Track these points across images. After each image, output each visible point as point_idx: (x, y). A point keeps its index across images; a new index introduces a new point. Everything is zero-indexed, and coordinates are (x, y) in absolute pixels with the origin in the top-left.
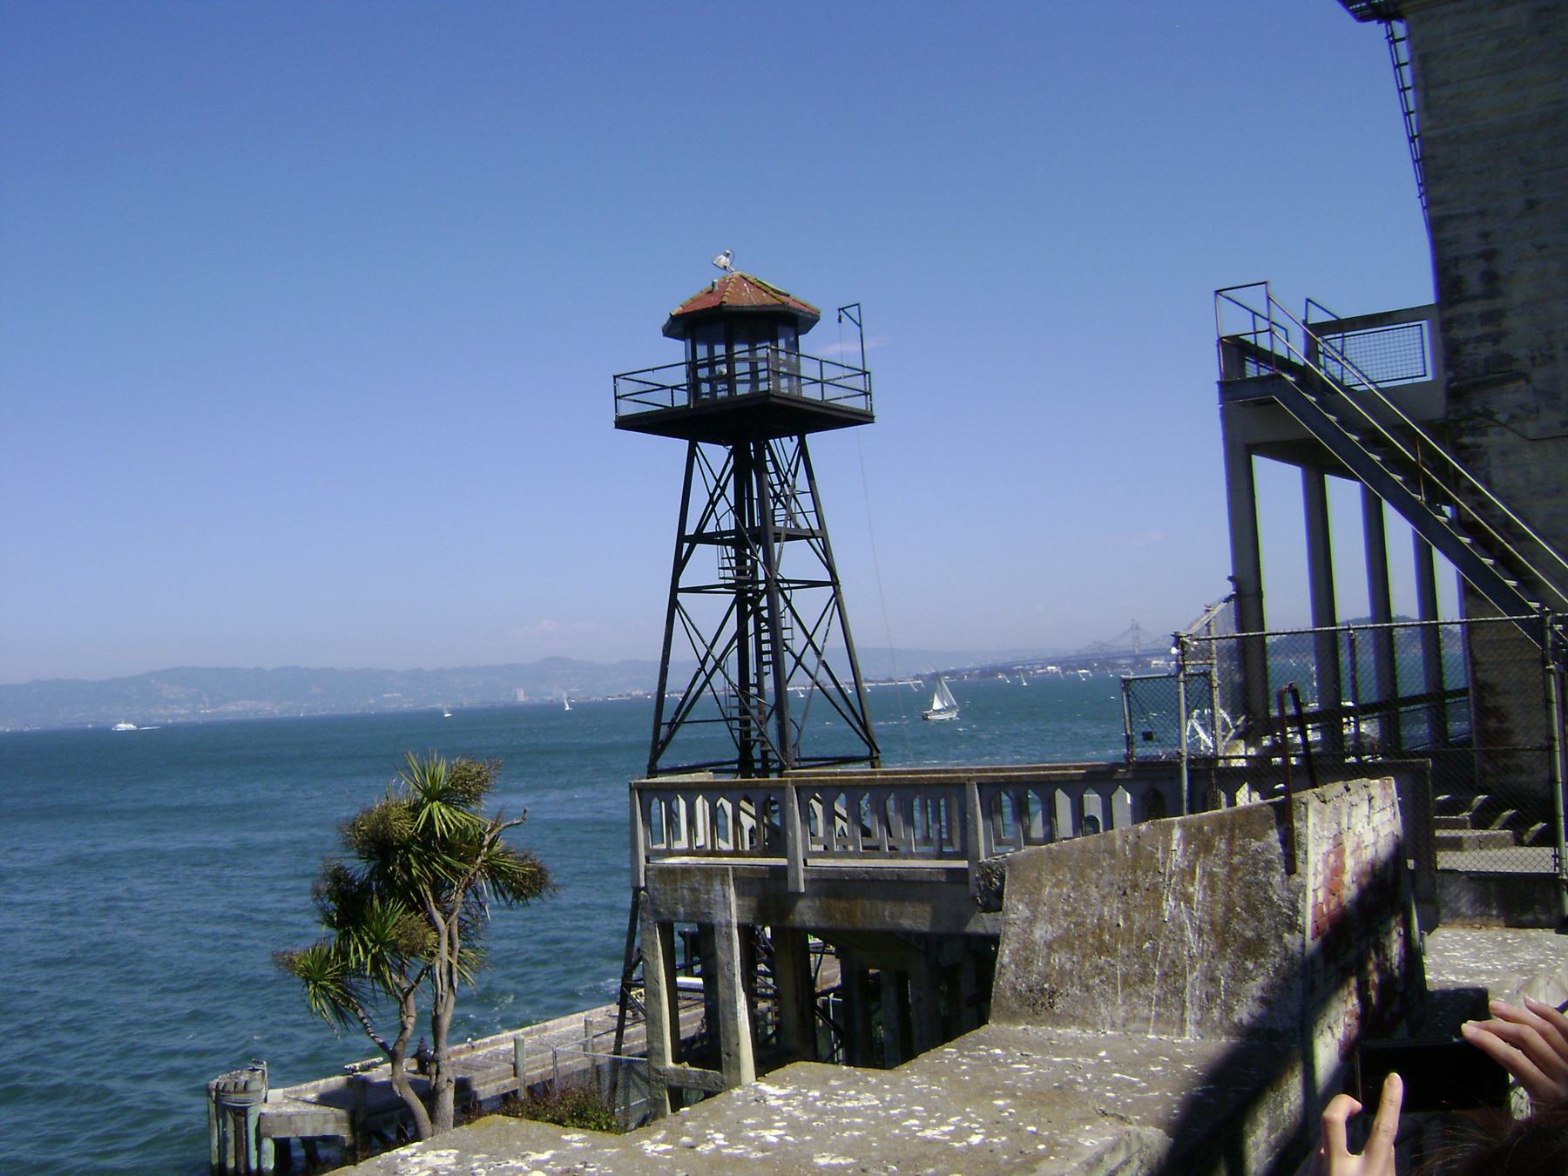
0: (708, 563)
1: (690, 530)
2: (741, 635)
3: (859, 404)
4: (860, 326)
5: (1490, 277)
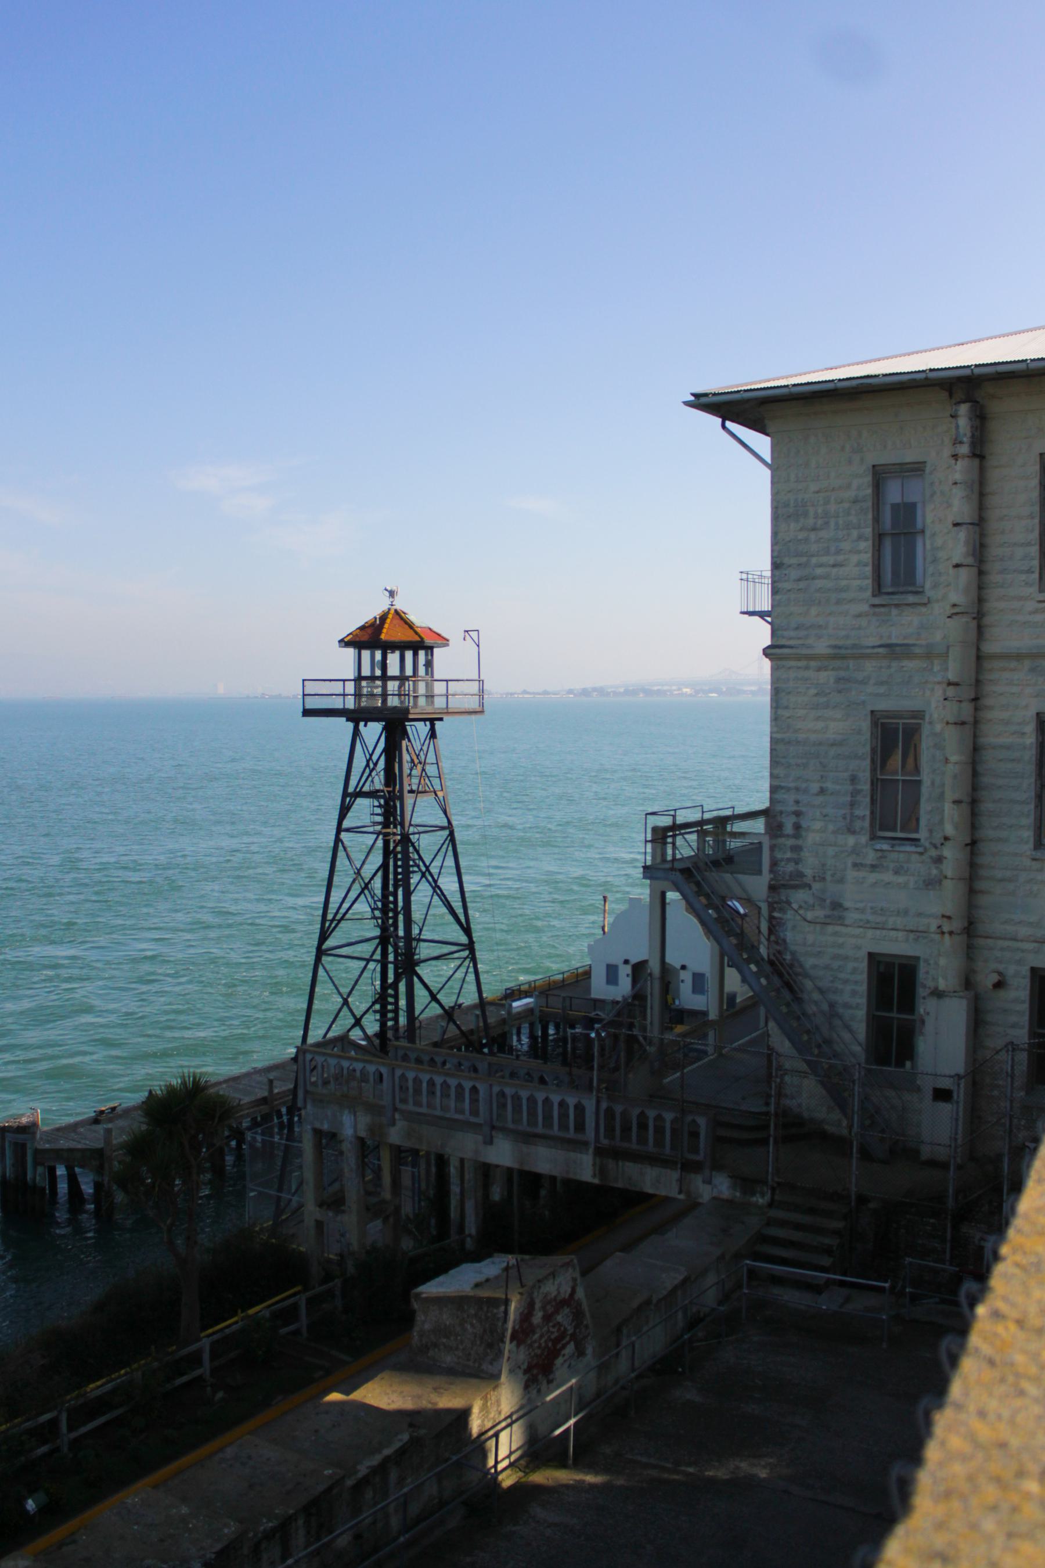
0: (364, 811)
1: (351, 790)
2: (384, 866)
3: (473, 704)
4: (478, 646)
5: (797, 827)
